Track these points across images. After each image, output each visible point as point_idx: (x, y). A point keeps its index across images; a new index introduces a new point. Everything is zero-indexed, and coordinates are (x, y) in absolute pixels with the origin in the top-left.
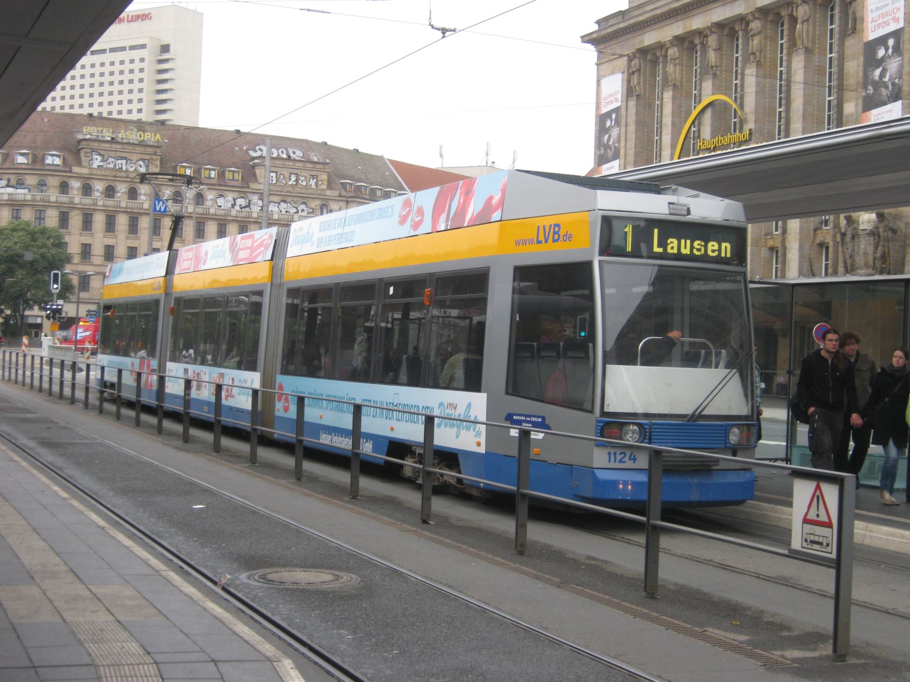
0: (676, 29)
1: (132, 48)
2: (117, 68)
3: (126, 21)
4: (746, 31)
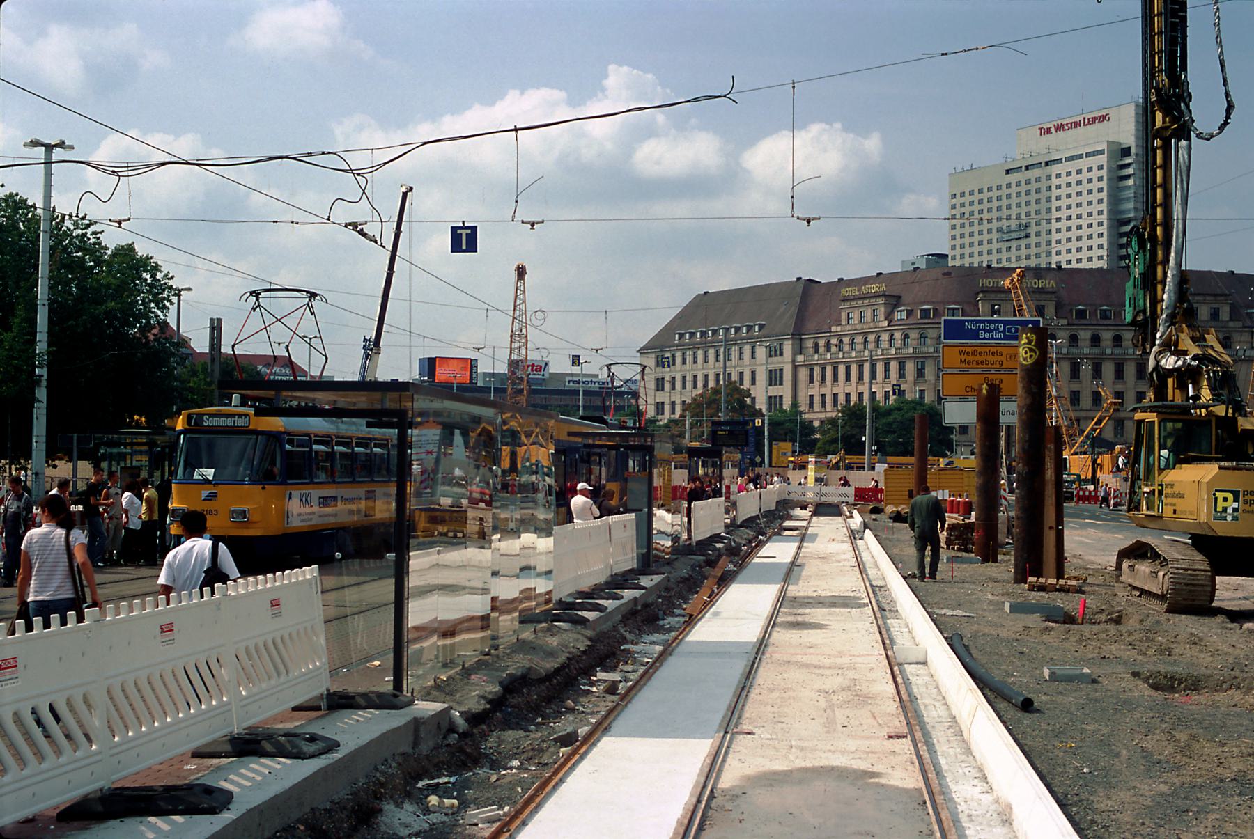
2: (1073, 179)
3: (1082, 125)
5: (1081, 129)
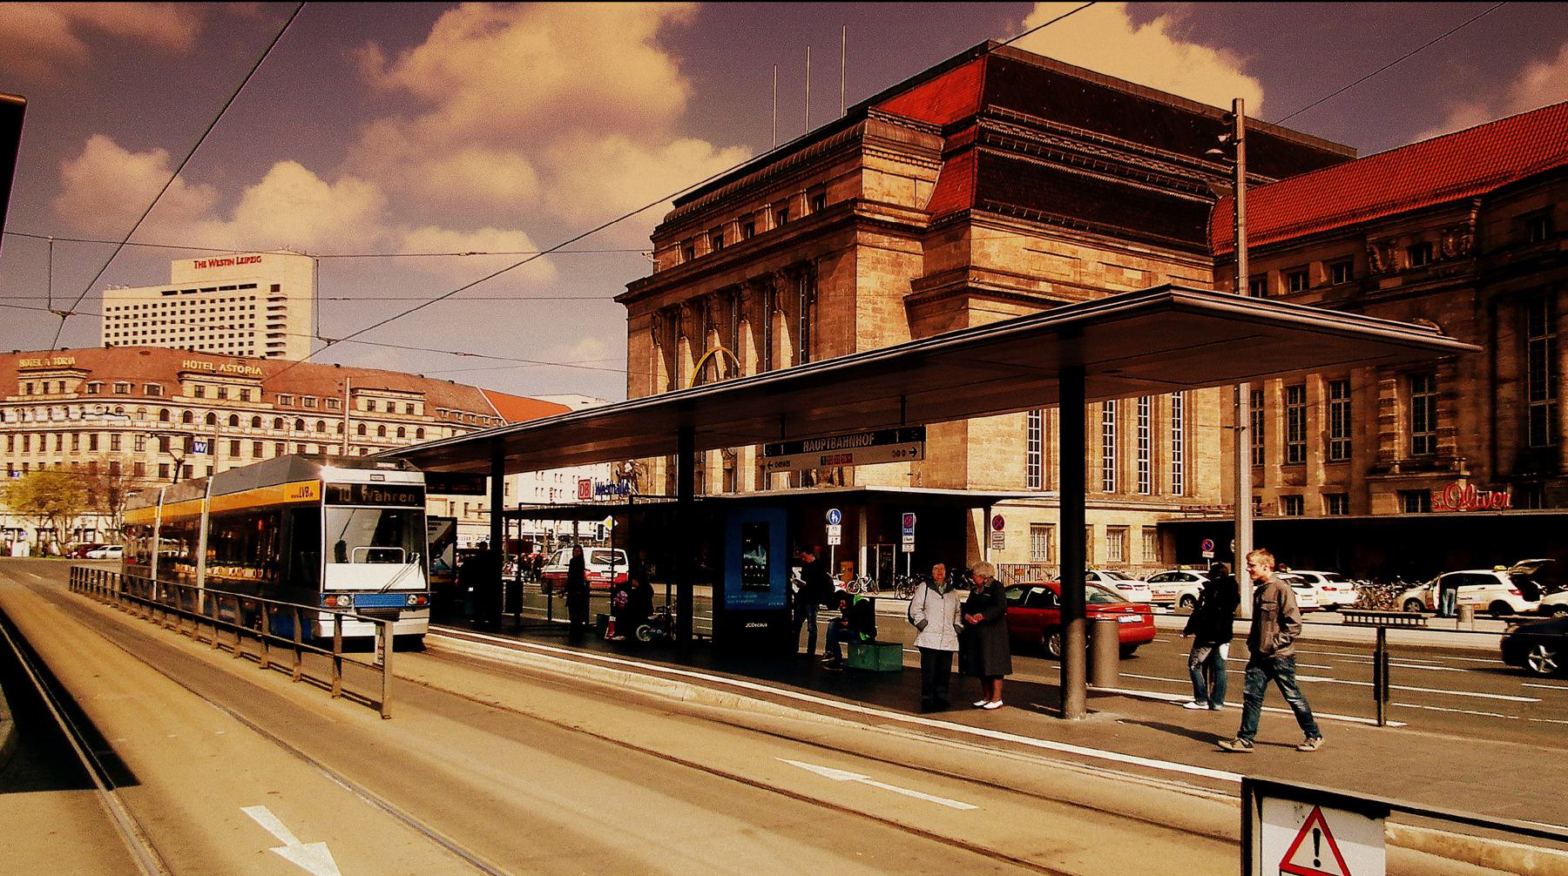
0: (687, 293)
1: (242, 287)
3: (235, 262)
4: (739, 298)
5: (235, 267)
